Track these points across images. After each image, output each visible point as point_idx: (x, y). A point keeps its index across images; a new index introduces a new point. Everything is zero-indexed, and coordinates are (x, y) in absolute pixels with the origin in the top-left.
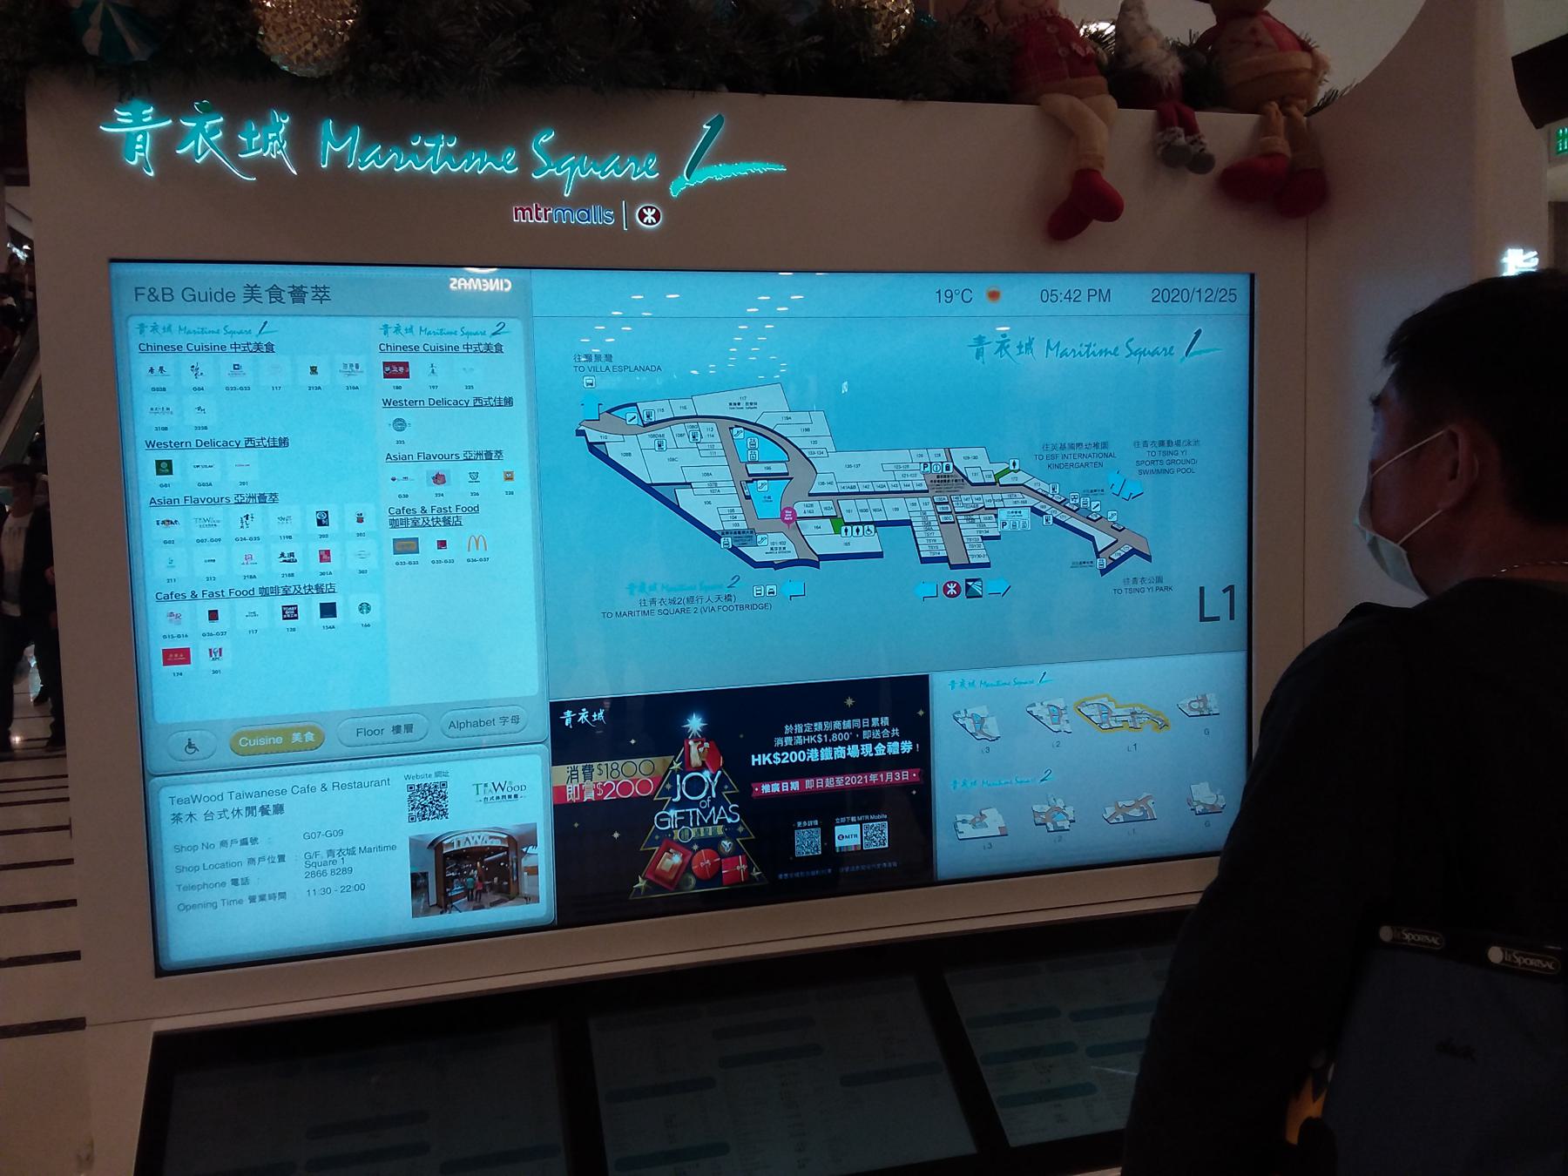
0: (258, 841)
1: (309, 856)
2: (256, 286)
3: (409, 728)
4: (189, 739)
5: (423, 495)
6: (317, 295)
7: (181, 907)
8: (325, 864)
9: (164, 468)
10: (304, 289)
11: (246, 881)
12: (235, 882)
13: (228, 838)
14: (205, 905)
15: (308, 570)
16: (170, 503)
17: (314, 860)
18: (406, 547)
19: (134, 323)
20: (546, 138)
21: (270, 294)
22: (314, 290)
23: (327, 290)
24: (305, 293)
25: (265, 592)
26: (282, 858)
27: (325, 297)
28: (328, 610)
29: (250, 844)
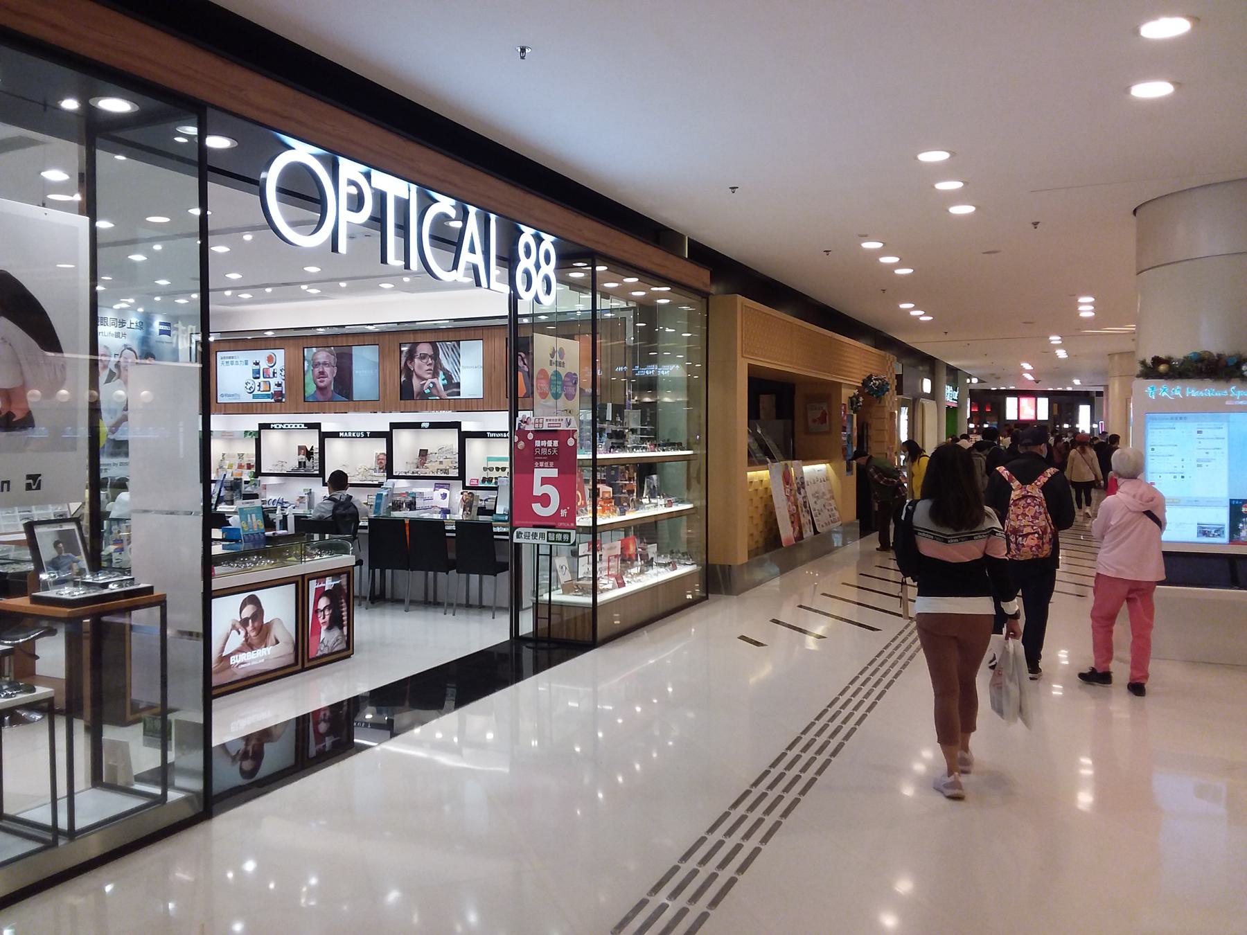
5: (1203, 455)
9: (1153, 449)
15: (1179, 469)
16: (1153, 456)
18: (1199, 466)
19: (1149, 424)
20: (1233, 388)
25: (1170, 473)
28: (1183, 477)
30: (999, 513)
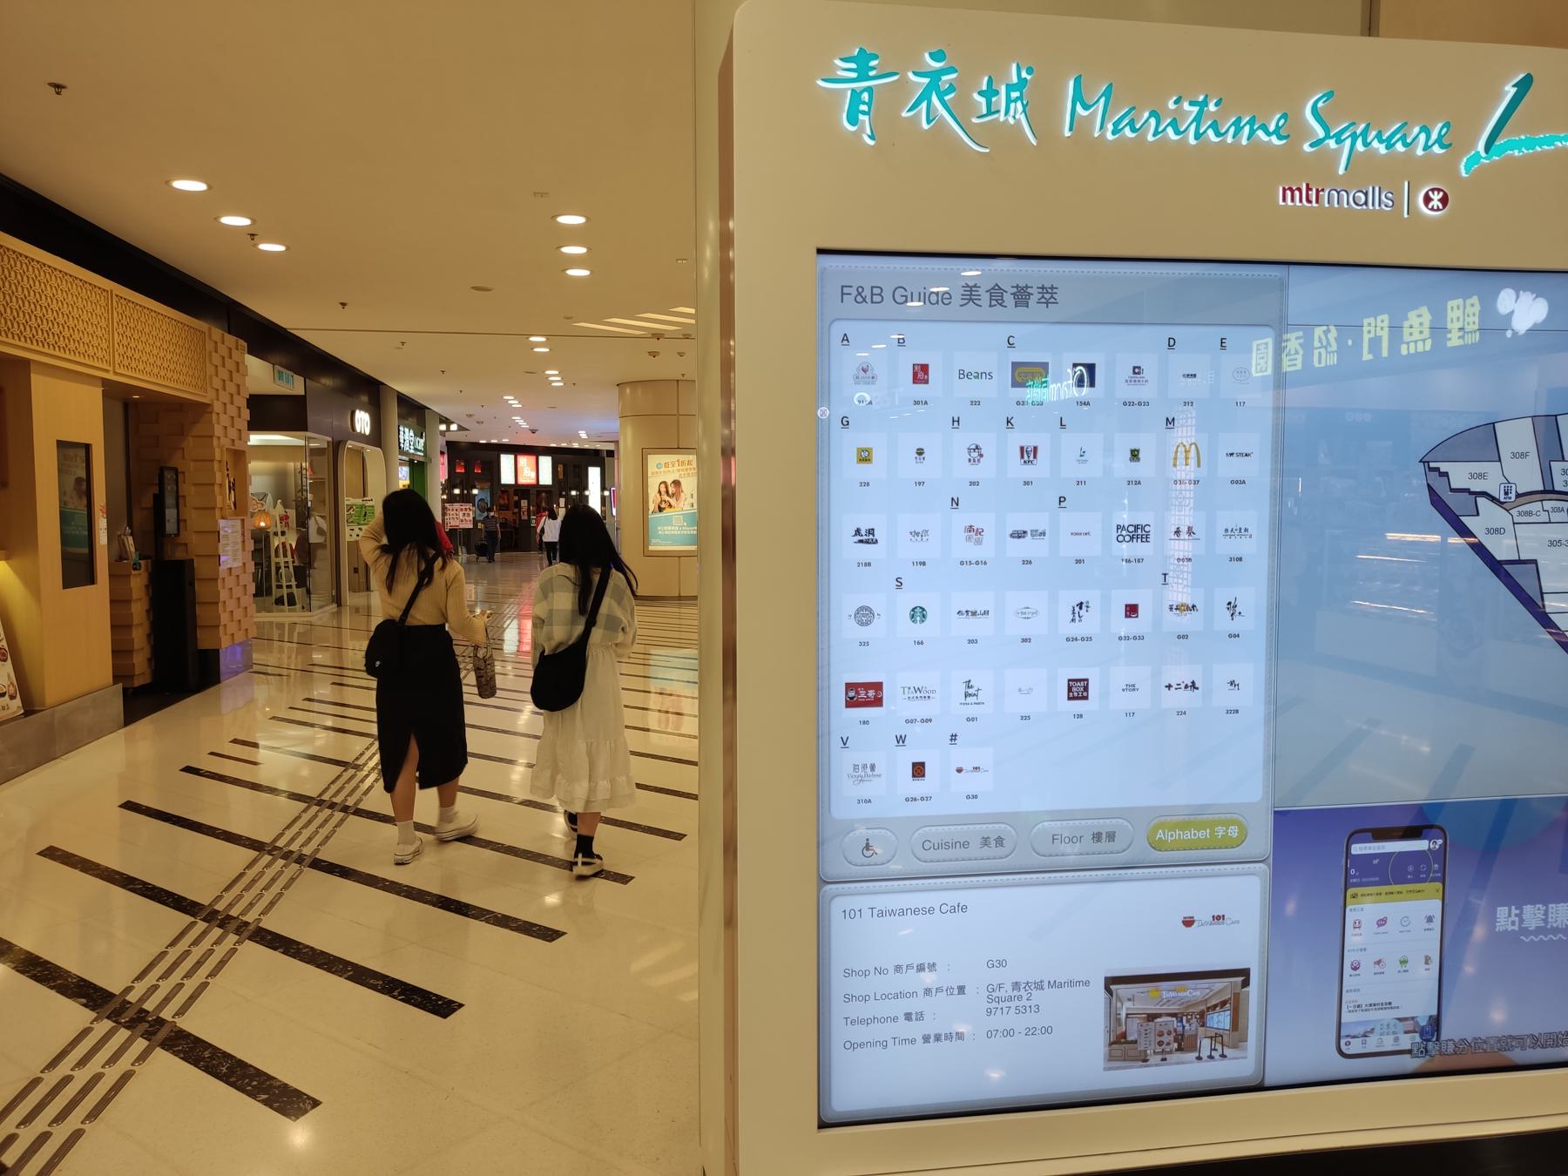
0: (937, 967)
1: (991, 989)
2: (975, 286)
3: (1111, 836)
4: (868, 840)
6: (1043, 297)
7: (848, 1045)
8: (1010, 999)
10: (1029, 290)
11: (920, 1016)
12: (908, 1016)
13: (904, 964)
14: (873, 1044)
17: (997, 994)
21: (991, 296)
22: (1040, 290)
23: (1055, 290)
24: (1030, 294)
26: (961, 990)
27: (1052, 300)
29: (927, 970)
30: (59, 853)
